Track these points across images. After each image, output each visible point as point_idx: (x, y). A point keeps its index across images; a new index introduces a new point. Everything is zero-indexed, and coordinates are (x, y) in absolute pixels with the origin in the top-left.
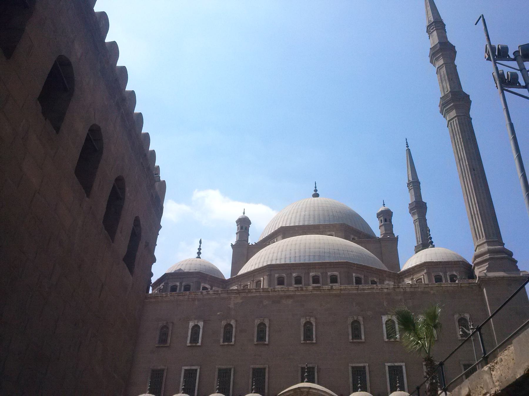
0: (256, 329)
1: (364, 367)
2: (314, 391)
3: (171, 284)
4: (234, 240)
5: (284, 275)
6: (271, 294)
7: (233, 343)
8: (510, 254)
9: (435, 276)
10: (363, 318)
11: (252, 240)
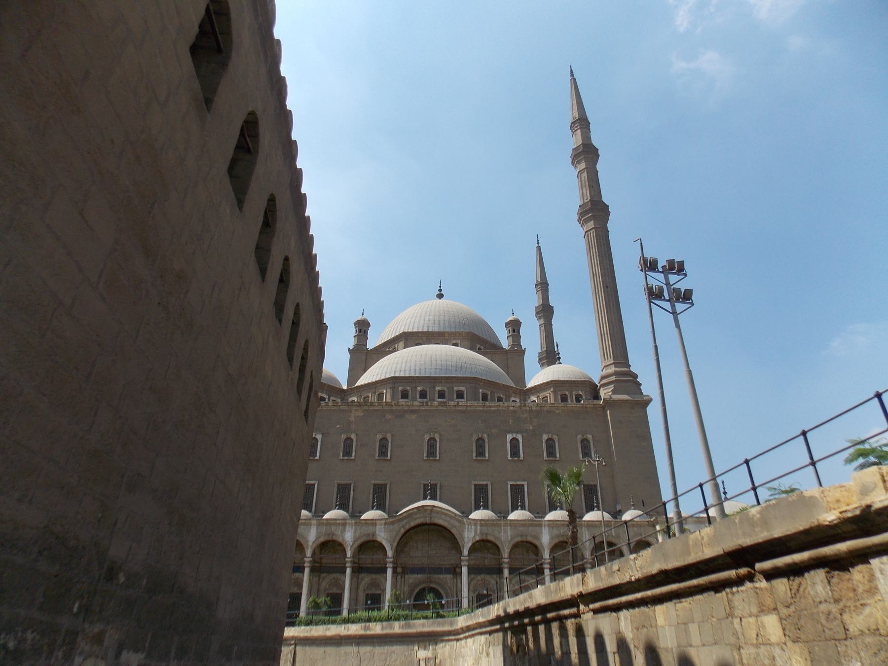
1: (487, 485)
4: (351, 343)
7: (353, 458)
8: (636, 376)
11: (371, 344)
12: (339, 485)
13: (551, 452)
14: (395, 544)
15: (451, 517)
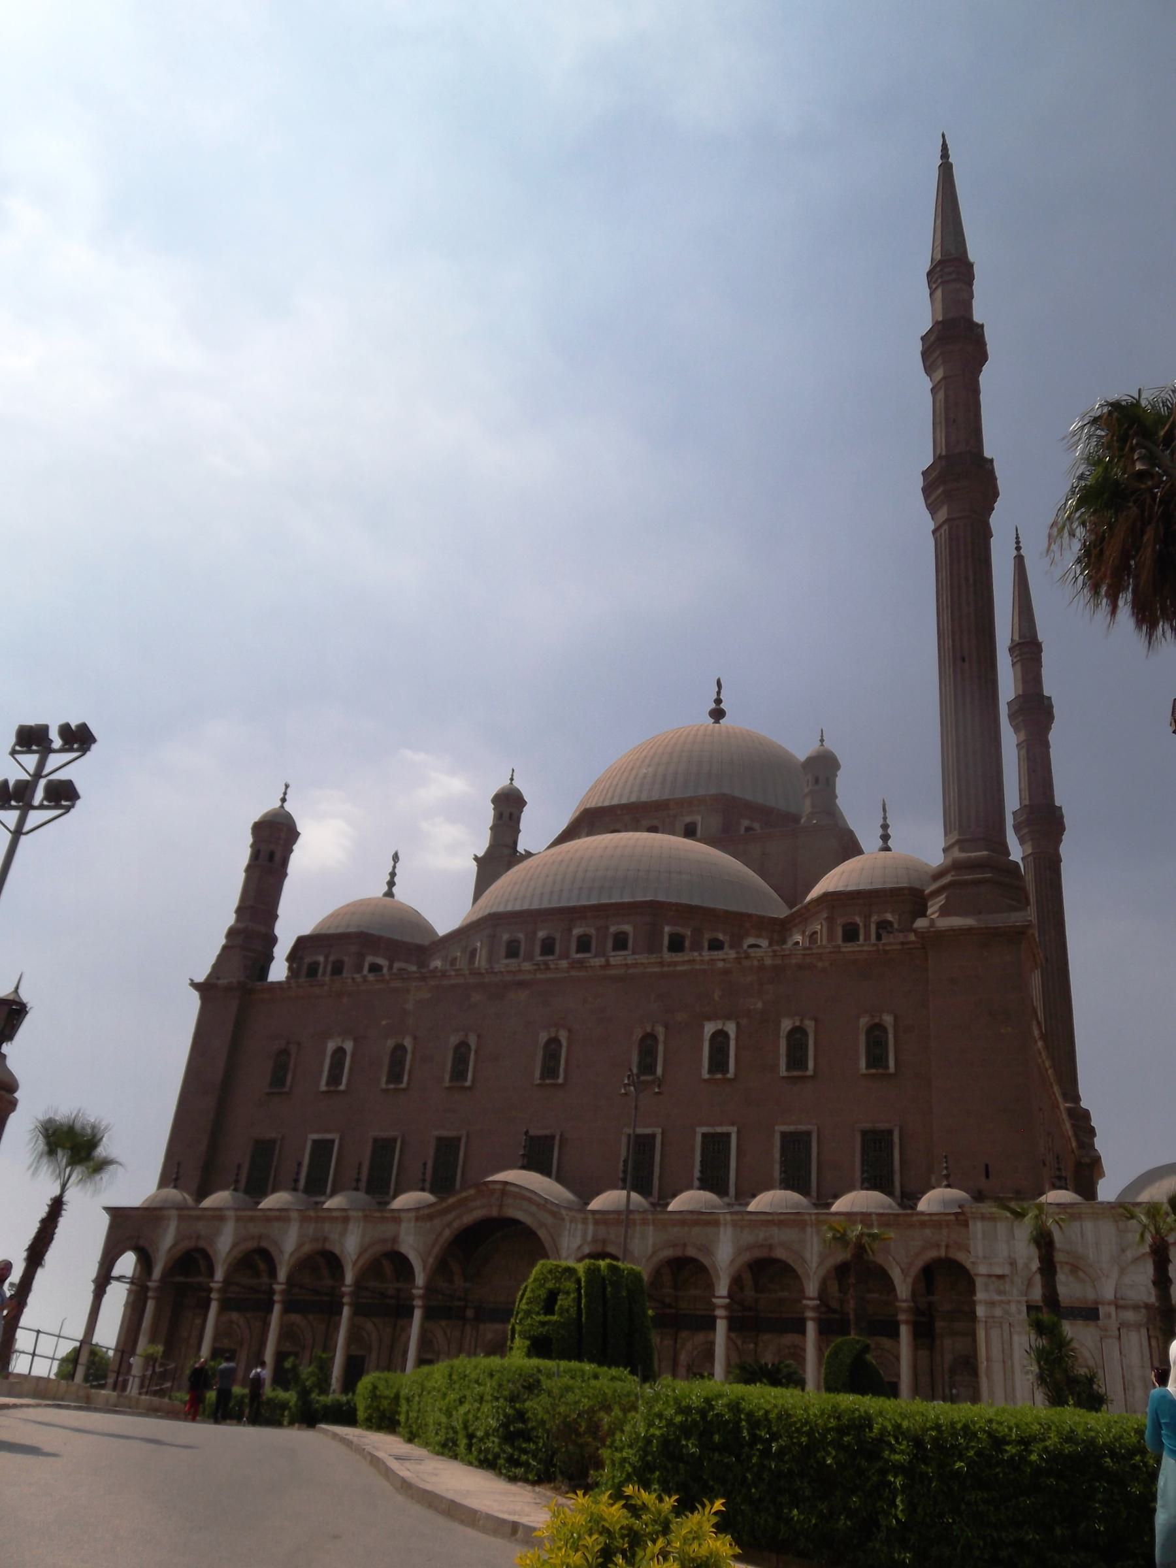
1: (653, 1136)
2: (513, 1189)
3: (308, 960)
5: (521, 936)
6: (486, 980)
9: (844, 926)
12: (376, 1140)
13: (796, 1059)
14: (431, 1260)
15: (538, 1205)
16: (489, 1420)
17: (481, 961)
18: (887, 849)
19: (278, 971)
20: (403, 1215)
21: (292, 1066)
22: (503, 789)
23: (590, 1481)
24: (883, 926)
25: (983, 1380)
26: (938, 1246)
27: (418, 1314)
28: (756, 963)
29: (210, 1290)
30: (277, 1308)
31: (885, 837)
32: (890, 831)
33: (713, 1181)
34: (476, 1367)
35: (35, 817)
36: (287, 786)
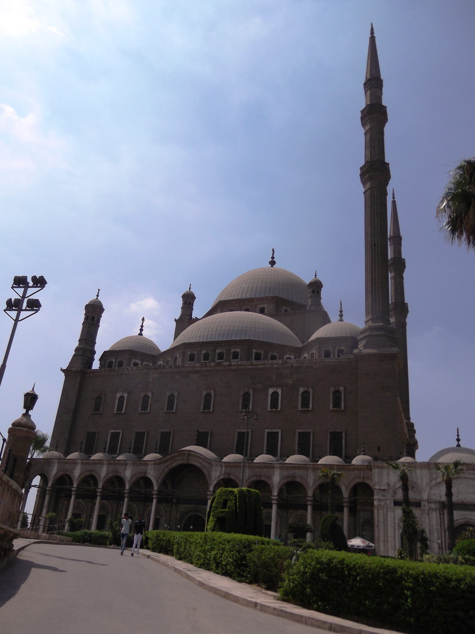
0: (167, 400)
2: (193, 453)
3: (108, 361)
4: (178, 314)
5: (195, 352)
10: (253, 390)
13: (305, 403)
14: (160, 480)
15: (203, 459)
16: (228, 559)
17: (179, 362)
18: (341, 320)
19: (96, 365)
20: (149, 463)
21: (102, 403)
22: (186, 292)
23: (279, 586)
24: (341, 351)
25: (376, 529)
26: (360, 478)
27: (155, 501)
28: (290, 365)
29: (72, 491)
30: (98, 498)
31: (341, 316)
32: (343, 313)
33: (272, 451)
34: (220, 537)
35: (23, 314)
36: (99, 290)
